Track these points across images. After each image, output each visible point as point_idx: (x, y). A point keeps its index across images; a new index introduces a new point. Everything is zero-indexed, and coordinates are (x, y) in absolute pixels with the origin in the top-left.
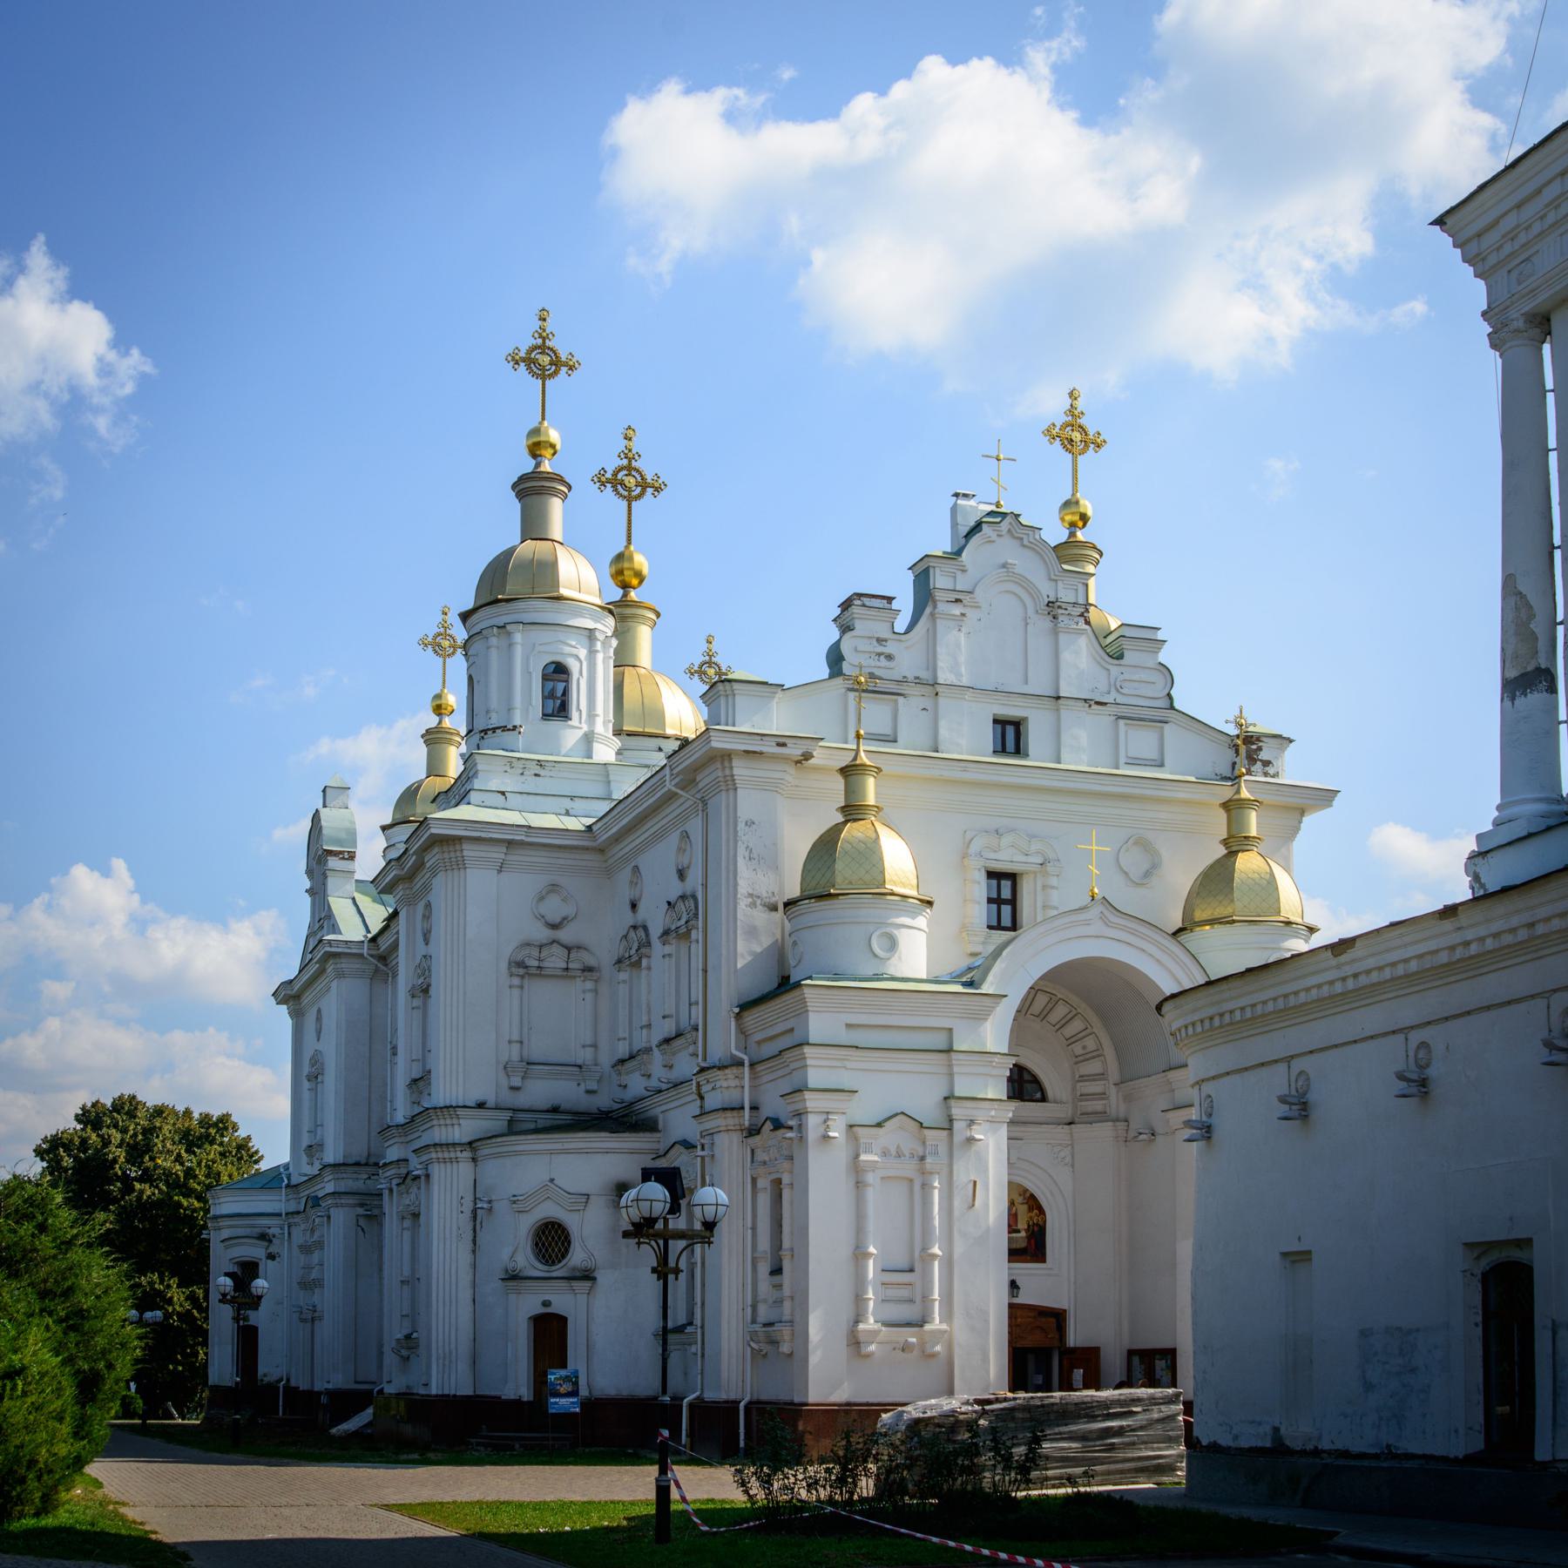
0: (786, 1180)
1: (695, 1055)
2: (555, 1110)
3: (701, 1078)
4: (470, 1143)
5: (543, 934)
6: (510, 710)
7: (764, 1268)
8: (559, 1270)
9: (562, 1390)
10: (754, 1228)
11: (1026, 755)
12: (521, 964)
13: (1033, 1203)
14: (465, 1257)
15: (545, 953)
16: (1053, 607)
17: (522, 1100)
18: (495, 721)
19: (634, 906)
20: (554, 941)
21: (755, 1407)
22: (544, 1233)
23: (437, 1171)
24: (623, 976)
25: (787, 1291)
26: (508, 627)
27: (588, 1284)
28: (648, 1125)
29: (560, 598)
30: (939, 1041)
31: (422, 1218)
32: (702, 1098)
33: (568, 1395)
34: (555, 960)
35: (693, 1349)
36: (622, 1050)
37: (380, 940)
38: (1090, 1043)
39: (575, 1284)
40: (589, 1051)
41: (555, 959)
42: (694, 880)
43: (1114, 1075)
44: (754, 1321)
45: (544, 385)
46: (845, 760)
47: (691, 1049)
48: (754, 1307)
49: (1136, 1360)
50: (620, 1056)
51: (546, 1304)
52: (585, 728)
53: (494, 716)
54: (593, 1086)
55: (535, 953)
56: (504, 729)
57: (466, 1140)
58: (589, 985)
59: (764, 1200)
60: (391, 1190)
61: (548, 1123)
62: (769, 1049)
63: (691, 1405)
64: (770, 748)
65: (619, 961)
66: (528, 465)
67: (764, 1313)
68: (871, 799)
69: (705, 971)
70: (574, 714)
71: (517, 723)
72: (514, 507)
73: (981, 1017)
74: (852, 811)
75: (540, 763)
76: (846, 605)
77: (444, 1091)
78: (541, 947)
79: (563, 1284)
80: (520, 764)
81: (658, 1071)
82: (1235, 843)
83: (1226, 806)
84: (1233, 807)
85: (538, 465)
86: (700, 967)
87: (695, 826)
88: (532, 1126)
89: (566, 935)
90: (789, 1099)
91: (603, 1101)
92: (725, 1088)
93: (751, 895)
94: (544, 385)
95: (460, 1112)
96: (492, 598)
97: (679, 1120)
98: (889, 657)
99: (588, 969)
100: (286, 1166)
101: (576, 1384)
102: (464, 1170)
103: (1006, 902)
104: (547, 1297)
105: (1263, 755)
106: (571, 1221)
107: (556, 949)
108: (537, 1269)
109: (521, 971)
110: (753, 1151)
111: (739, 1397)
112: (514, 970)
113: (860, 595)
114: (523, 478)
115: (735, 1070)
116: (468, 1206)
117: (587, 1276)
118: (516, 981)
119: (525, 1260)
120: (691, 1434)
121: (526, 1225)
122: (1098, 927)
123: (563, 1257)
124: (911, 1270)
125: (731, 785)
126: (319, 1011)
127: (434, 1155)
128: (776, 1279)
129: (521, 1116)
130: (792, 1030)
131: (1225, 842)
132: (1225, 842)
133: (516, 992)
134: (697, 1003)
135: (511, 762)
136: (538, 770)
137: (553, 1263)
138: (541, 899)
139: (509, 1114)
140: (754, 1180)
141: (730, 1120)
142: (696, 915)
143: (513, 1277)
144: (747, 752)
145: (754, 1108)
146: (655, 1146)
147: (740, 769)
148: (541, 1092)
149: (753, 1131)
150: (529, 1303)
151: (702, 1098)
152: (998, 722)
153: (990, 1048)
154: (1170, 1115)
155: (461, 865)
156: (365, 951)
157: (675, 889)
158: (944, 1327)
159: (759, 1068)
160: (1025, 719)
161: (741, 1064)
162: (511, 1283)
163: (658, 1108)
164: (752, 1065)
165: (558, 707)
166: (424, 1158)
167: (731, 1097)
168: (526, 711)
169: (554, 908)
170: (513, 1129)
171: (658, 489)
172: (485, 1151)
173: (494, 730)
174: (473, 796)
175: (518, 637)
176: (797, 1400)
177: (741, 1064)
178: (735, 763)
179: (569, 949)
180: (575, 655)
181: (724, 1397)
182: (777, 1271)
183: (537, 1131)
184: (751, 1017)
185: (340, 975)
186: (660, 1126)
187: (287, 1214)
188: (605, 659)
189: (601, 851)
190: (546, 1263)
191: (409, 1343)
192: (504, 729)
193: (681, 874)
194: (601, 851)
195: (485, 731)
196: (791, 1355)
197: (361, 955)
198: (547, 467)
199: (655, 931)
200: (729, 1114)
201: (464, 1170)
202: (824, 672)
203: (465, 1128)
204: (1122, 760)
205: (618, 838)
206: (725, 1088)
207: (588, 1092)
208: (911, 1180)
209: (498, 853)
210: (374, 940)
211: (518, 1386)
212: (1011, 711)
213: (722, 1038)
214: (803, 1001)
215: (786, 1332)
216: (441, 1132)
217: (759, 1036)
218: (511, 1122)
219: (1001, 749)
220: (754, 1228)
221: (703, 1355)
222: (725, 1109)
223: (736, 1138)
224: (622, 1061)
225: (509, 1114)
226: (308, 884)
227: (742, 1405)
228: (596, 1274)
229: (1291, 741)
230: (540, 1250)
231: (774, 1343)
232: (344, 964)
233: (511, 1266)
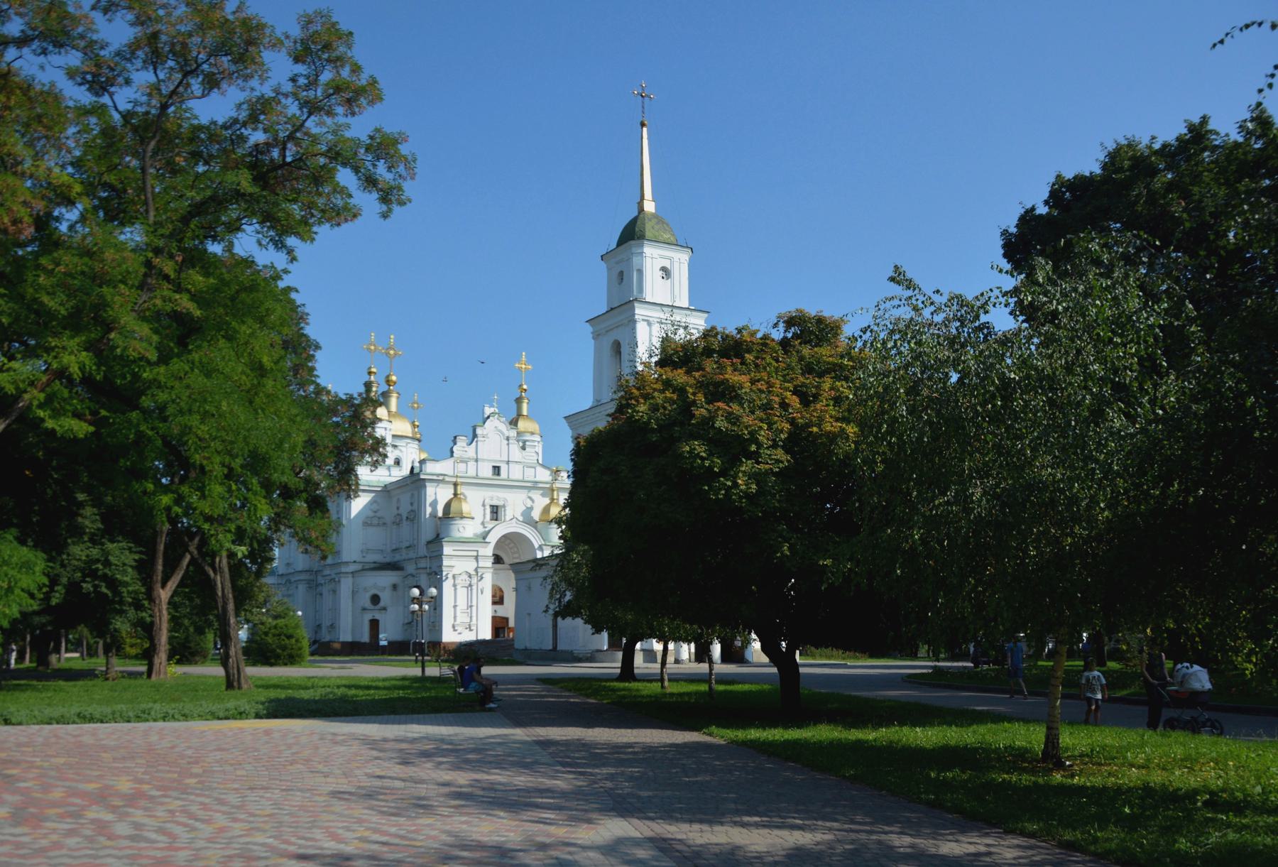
5: (372, 514)
8: (378, 607)
13: (501, 590)
23: (343, 580)
30: (475, 554)
36: (394, 547)
42: (415, 507)
81: (404, 556)
87: (416, 493)
89: (378, 514)
92: (422, 564)
99: (384, 524)
117: (384, 609)
119: (368, 604)
121: (368, 595)
125: (425, 487)
143: (364, 609)
150: (368, 617)
152: (494, 467)
157: (410, 508)
184: (430, 546)
191: (332, 627)
193: (412, 504)
203: (352, 568)
206: (422, 564)
211: (365, 638)
213: (423, 551)
219: (494, 474)
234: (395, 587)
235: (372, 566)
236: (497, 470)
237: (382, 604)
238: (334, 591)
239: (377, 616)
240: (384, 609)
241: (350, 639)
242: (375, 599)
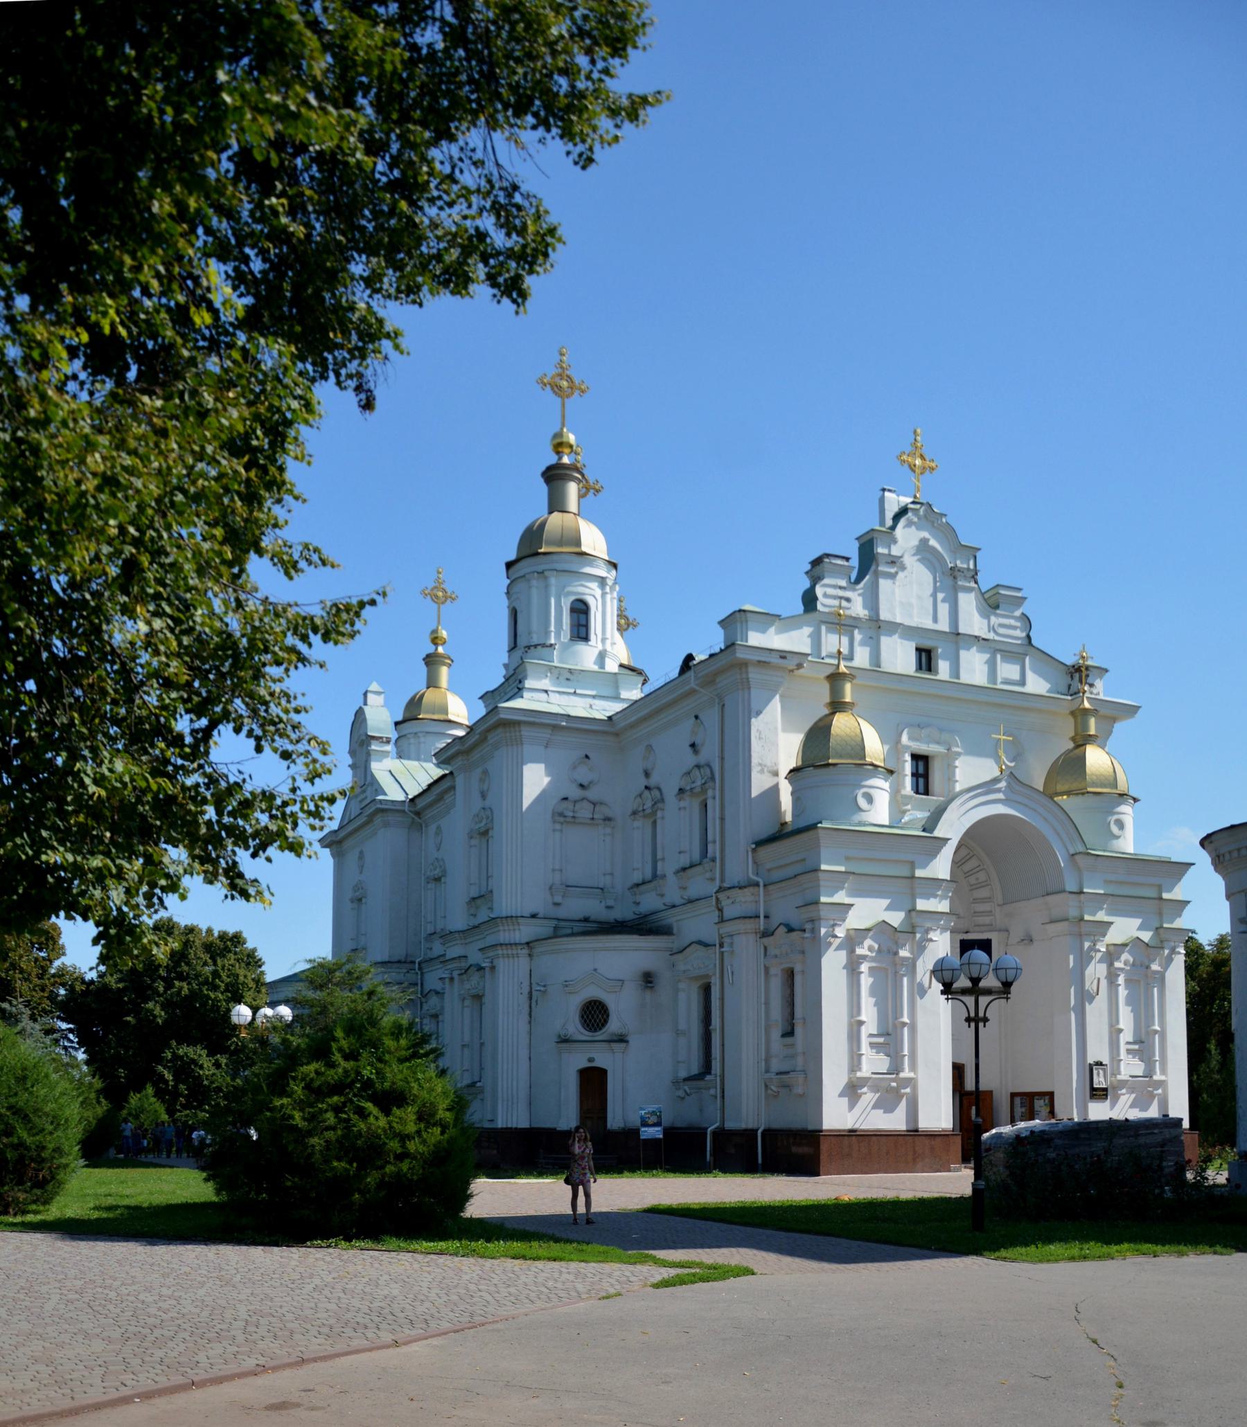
0: (797, 969)
1: (712, 879)
2: (586, 920)
3: (722, 896)
4: (528, 943)
5: (575, 793)
6: (547, 633)
7: (776, 1034)
8: (600, 1035)
9: (650, 1122)
10: (767, 1003)
11: (937, 673)
12: (561, 814)
14: (524, 1027)
15: (578, 806)
16: (954, 572)
17: (562, 913)
18: (535, 641)
19: (647, 774)
20: (583, 799)
21: (769, 1133)
23: (502, 965)
24: (636, 824)
25: (800, 1047)
26: (546, 573)
27: (623, 1045)
28: (665, 931)
29: (585, 554)
31: (486, 1000)
32: (720, 910)
33: (654, 1125)
34: (584, 811)
35: (712, 1092)
37: (417, 801)
38: (982, 876)
39: (613, 1045)
40: (608, 877)
41: (584, 811)
43: (999, 898)
44: (767, 1071)
45: (563, 405)
46: (830, 670)
47: (708, 875)
48: (767, 1061)
49: (1018, 1100)
50: (636, 881)
51: (591, 1060)
52: (600, 647)
53: (535, 636)
54: (611, 903)
55: (571, 807)
56: (544, 645)
57: (524, 941)
58: (608, 830)
59: (776, 984)
60: (452, 979)
61: (581, 930)
62: (777, 875)
63: (714, 1133)
64: (775, 660)
65: (634, 813)
66: (552, 459)
67: (776, 1065)
68: (848, 698)
69: (722, 819)
70: (592, 636)
71: (553, 641)
72: (543, 489)
73: (934, 853)
74: (837, 706)
75: (570, 671)
76: (817, 562)
77: (506, 903)
78: (575, 802)
79: (604, 1045)
80: (556, 671)
82: (1082, 740)
83: (1073, 713)
84: (1080, 715)
85: (560, 458)
86: (718, 815)
88: (569, 931)
89: (592, 794)
90: (803, 909)
91: (623, 912)
92: (742, 902)
93: (760, 764)
94: (563, 405)
95: (521, 920)
96: (532, 551)
97: (696, 925)
98: (848, 600)
99: (608, 819)
101: (660, 1117)
102: (523, 963)
103: (921, 776)
105: (1090, 680)
107: (585, 804)
108: (582, 1034)
109: (562, 819)
110: (766, 948)
111: (755, 1127)
112: (557, 818)
113: (828, 555)
114: (549, 469)
115: (751, 889)
116: (526, 990)
117: (622, 1039)
118: (558, 826)
119: (574, 1027)
120: (714, 1154)
121: (575, 1003)
123: (603, 1025)
125: (746, 685)
126: (361, 853)
127: (500, 952)
128: (789, 1040)
129: (563, 924)
130: (804, 860)
131: (1073, 739)
132: (1073, 739)
133: (557, 834)
134: (714, 842)
135: (551, 668)
136: (569, 676)
137: (595, 1031)
138: (575, 768)
139: (555, 922)
140: (767, 969)
141: (749, 925)
142: (713, 778)
143: (564, 1040)
144: (759, 662)
145: (766, 917)
146: (670, 945)
147: (754, 674)
148: (578, 907)
149: (766, 934)
151: (720, 910)
153: (940, 877)
154: (1047, 926)
155: (519, 742)
156: (406, 808)
157: (690, 759)
158: (912, 1075)
159: (770, 888)
161: (757, 885)
162: (564, 1045)
163: (671, 918)
164: (765, 886)
165: (581, 631)
166: (491, 954)
167: (749, 909)
168: (558, 635)
169: (583, 775)
170: (556, 934)
171: (598, 491)
172: (539, 949)
173: (535, 646)
174: (526, 694)
175: (553, 581)
176: (810, 1127)
177: (757, 885)
178: (751, 669)
179: (594, 804)
180: (592, 593)
181: (744, 1126)
182: (789, 1033)
183: (573, 935)
184: (767, 852)
185: (386, 825)
186: (675, 931)
188: (612, 599)
189: (617, 735)
190: (590, 1030)
192: (544, 645)
194: (617, 735)
195: (529, 647)
196: (801, 1096)
197: (404, 811)
198: (566, 460)
199: (670, 792)
200: (747, 921)
201: (523, 963)
202: (801, 608)
203: (526, 931)
204: (999, 680)
205: (632, 726)
206: (742, 902)
207: (608, 907)
208: (886, 970)
209: (545, 734)
210: (412, 800)
212: (927, 644)
213: (739, 865)
214: (818, 839)
215: (801, 1078)
216: (505, 934)
217: (768, 866)
218: (556, 928)
219: (920, 667)
220: (767, 1003)
221: (723, 1097)
222: (745, 917)
223: (752, 938)
224: (638, 885)
225: (555, 922)
226: (350, 761)
227: (759, 1132)
228: (629, 1038)
229: (1107, 671)
231: (787, 1086)
232: (391, 818)
233: (562, 1033)
234: (648, 979)
235: (579, 927)
236: (926, 659)
237: (613, 1026)
238: (478, 998)
240: (622, 1039)
241: (523, 1123)
242: (595, 1014)
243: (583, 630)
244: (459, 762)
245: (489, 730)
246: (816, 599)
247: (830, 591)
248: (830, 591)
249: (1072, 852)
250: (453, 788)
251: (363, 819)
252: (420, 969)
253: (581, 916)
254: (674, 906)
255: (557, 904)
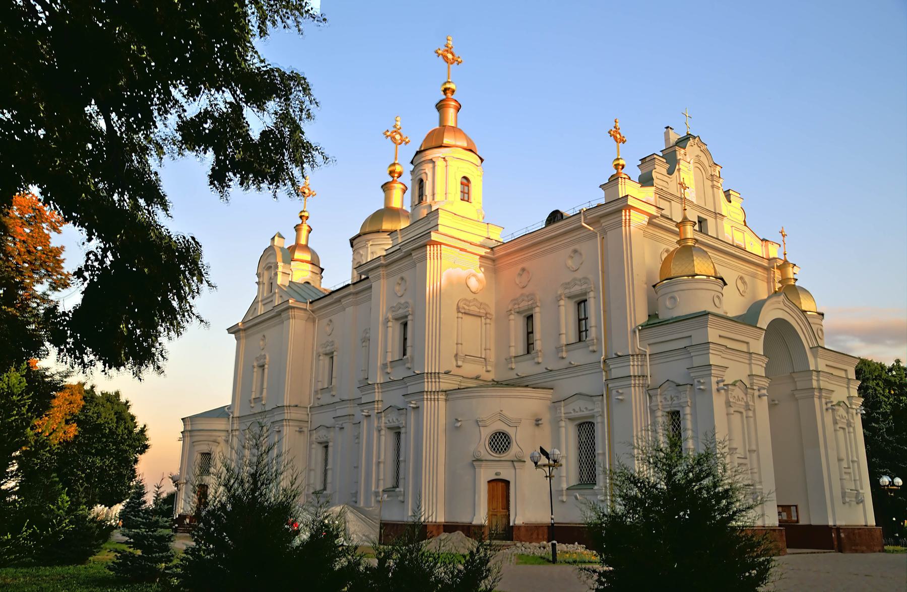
2: (477, 378)
22: (494, 437)
23: (427, 405)
51: (497, 474)
70: (472, 199)
100: (229, 407)
104: (498, 471)
106: (510, 431)
110: (650, 396)
119: (484, 451)
121: (486, 433)
122: (782, 306)
124: (746, 458)
150: (486, 474)
160: (706, 220)
187: (232, 430)
189: (493, 260)
203: (446, 384)
207: (488, 371)
230: (492, 446)
237: (514, 450)
239: (506, 473)
242: (501, 441)
243: (466, 196)
244: (381, 271)
245: (414, 250)
246: (653, 179)
247: (660, 176)
248: (660, 176)
249: (811, 346)
250: (371, 287)
251: (273, 314)
252: (310, 411)
253: (474, 376)
254: (551, 371)
255: (459, 367)
